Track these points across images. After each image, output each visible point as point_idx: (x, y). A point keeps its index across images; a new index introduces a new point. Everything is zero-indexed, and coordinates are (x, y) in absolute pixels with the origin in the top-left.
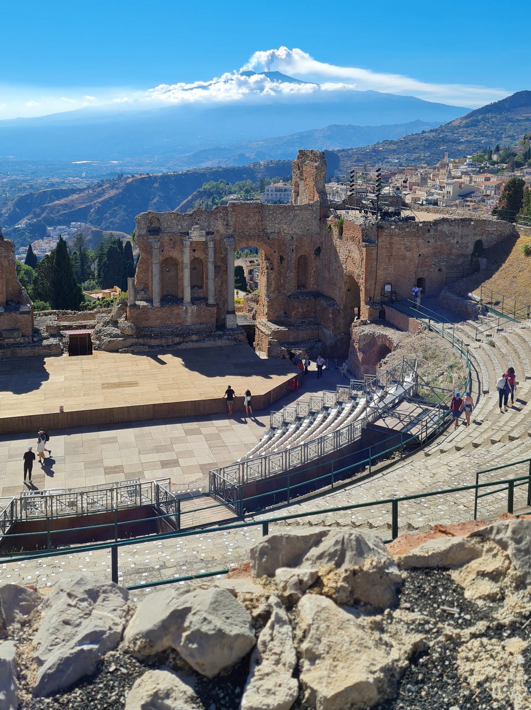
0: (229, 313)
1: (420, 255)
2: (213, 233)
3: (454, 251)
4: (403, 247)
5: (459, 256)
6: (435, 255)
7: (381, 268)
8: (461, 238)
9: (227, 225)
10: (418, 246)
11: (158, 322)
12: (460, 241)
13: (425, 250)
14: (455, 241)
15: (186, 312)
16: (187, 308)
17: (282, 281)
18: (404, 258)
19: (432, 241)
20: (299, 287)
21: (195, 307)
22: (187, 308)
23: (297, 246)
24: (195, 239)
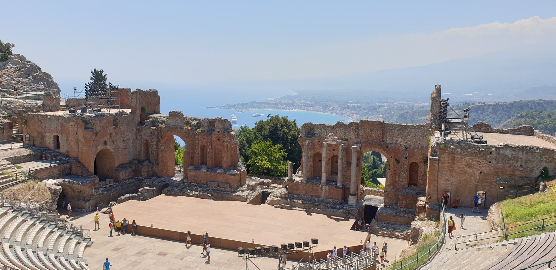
0: (352, 195)
1: (481, 172)
2: (347, 140)
3: (517, 173)
4: (464, 164)
5: (522, 178)
6: (496, 174)
7: (443, 178)
8: (526, 162)
9: (358, 135)
10: (479, 164)
11: (304, 192)
12: (524, 165)
13: (486, 169)
14: (519, 164)
15: (322, 189)
16: (322, 186)
17: (397, 179)
18: (465, 173)
19: (494, 162)
20: (410, 184)
21: (327, 187)
22: (322, 186)
23: (409, 155)
24: (329, 142)
